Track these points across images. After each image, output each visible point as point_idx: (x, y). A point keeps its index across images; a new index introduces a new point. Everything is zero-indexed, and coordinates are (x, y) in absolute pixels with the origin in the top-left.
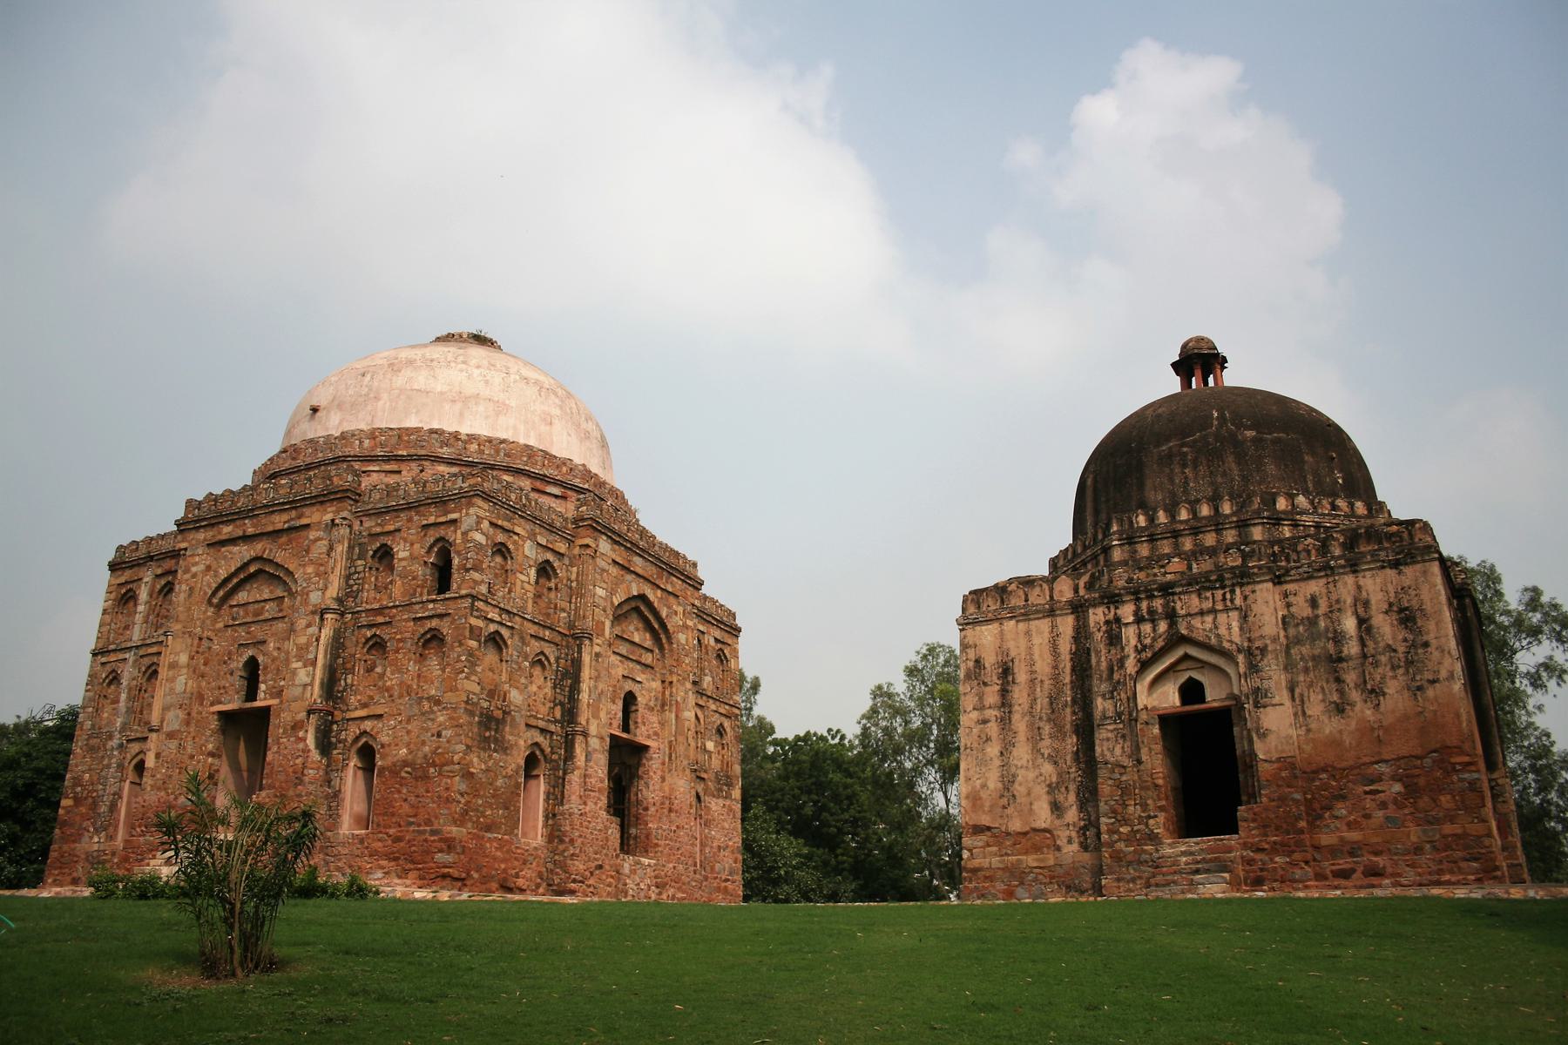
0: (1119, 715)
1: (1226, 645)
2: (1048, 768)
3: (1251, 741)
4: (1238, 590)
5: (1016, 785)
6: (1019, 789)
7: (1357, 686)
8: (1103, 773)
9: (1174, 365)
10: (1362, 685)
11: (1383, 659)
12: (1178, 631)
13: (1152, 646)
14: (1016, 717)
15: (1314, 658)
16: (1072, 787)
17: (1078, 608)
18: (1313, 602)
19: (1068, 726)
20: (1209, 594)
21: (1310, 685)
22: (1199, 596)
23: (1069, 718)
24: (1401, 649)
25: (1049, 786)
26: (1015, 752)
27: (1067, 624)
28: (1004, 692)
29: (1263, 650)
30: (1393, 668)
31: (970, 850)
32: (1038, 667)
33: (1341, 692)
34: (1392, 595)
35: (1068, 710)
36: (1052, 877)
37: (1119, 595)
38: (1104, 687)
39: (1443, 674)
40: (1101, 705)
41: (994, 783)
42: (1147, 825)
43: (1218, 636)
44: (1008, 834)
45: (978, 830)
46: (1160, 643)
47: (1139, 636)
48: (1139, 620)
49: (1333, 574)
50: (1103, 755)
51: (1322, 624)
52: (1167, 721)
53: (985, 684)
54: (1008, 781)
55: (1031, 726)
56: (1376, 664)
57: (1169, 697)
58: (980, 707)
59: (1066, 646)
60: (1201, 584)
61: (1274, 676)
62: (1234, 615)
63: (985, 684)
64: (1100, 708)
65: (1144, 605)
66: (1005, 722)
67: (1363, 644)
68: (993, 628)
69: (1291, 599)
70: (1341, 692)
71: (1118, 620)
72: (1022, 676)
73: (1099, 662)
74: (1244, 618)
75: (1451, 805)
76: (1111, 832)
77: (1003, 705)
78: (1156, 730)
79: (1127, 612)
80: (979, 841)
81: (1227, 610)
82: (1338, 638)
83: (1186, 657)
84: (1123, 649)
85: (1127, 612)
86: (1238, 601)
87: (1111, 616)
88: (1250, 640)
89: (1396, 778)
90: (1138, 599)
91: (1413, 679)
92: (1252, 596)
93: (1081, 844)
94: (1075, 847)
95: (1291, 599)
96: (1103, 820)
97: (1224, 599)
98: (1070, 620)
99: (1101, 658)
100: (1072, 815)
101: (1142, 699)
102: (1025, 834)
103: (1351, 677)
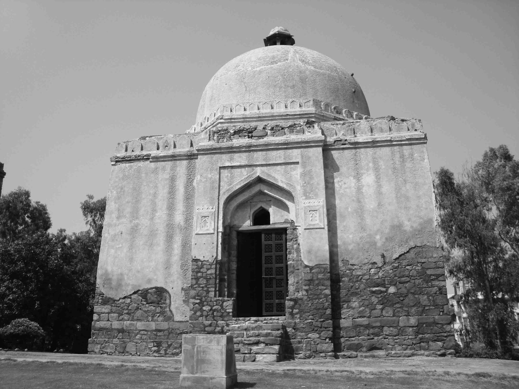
9: (265, 40)
80: (106, 309)
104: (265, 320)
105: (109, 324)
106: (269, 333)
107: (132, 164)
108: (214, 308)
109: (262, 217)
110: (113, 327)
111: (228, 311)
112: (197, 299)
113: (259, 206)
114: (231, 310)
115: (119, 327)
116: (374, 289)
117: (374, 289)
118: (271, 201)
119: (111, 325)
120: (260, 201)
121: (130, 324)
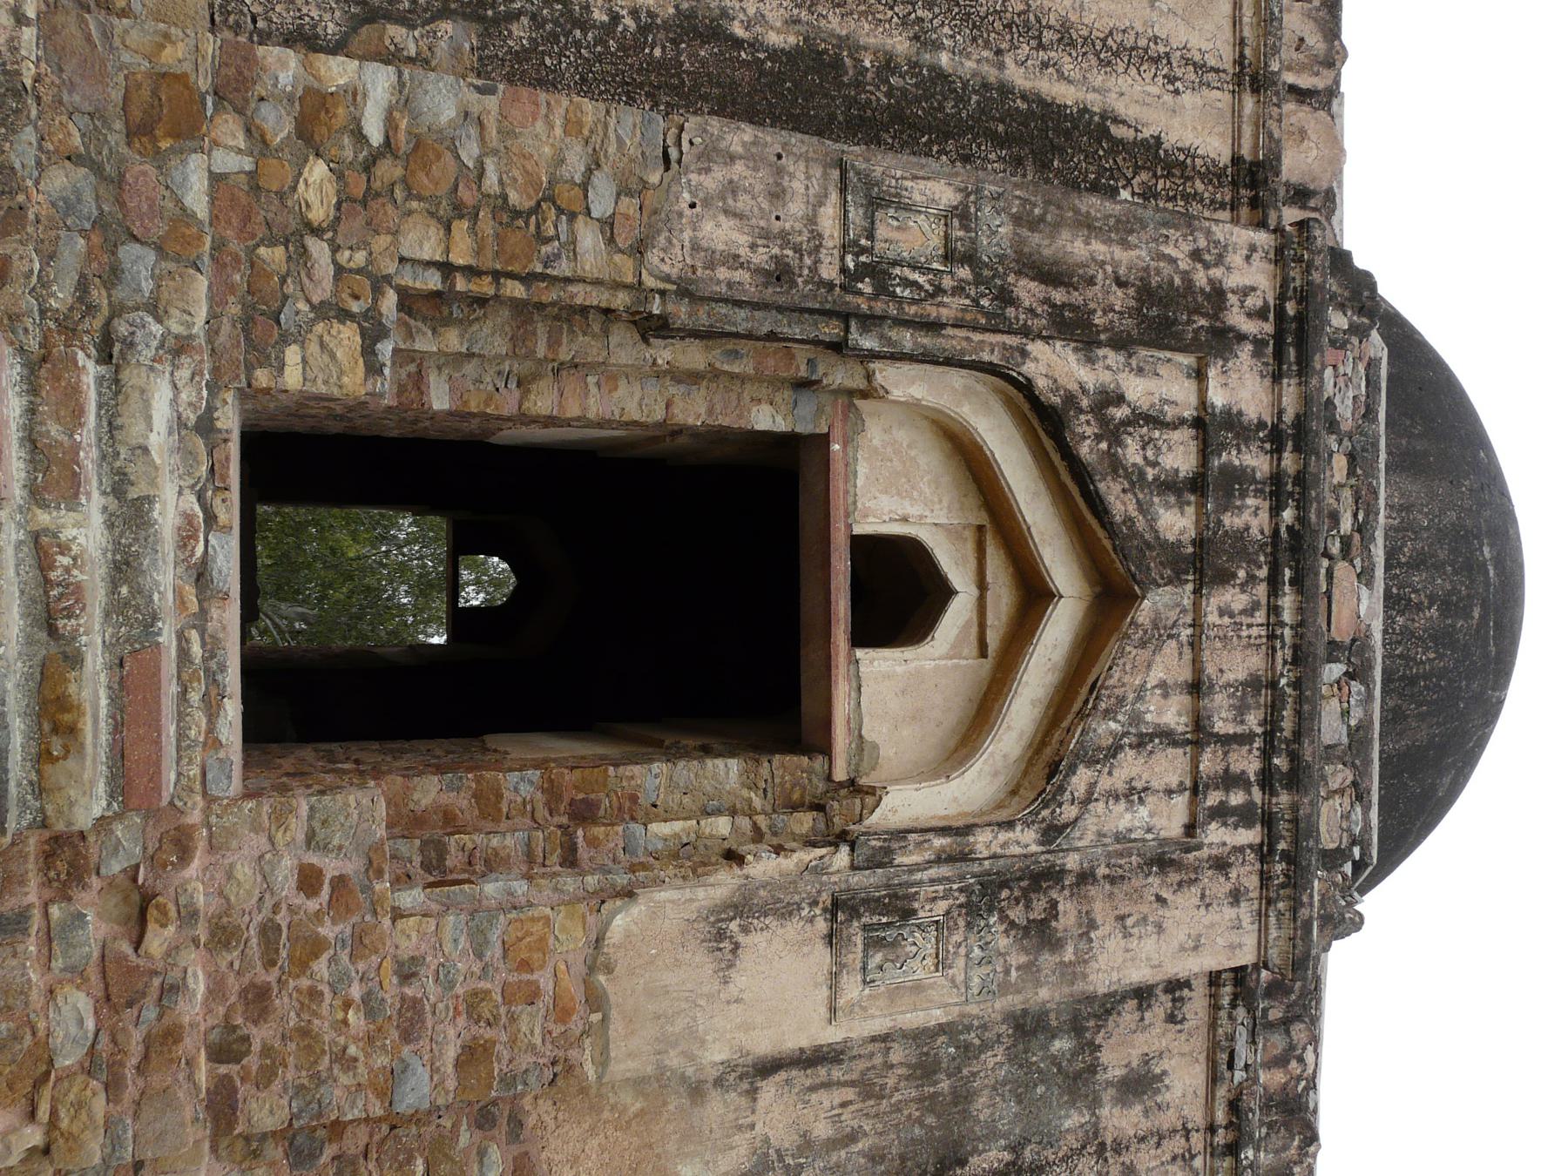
0: (878, 272)
1: (1081, 779)
3: (691, 859)
4: (1249, 836)
8: (630, 128)
12: (1148, 584)
13: (1115, 465)
15: (962, 1097)
18: (1140, 1084)
19: (834, 23)
20: (1253, 721)
21: (868, 1089)
22: (1252, 684)
27: (1198, 126)
29: (1041, 934)
35: (900, 44)
37: (1304, 369)
38: (996, 233)
40: (926, 197)
43: (1115, 750)
46: (1119, 501)
47: (1151, 419)
48: (1208, 427)
49: (1213, 1151)
50: (711, 155)
51: (1074, 1119)
57: (888, 488)
60: (1285, 699)
61: (939, 983)
62: (1170, 818)
64: (918, 191)
65: (1256, 461)
69: (1161, 1005)
71: (1222, 341)
73: (1087, 225)
74: (1161, 861)
76: (316, 116)
78: (766, 418)
79: (1242, 388)
81: (1196, 789)
83: (1034, 596)
84: (1121, 343)
85: (1242, 388)
86: (1216, 835)
87: (1237, 319)
88: (1086, 877)
90: (1276, 438)
92: (1219, 887)
95: (1161, 1005)
96: (379, 82)
97: (1230, 780)
98: (1214, 146)
99: (1105, 250)
101: (907, 384)
108: (318, 249)
109: (898, 593)
111: (292, 354)
112: (390, 124)
114: (293, 378)
118: (983, 653)
120: (982, 585)
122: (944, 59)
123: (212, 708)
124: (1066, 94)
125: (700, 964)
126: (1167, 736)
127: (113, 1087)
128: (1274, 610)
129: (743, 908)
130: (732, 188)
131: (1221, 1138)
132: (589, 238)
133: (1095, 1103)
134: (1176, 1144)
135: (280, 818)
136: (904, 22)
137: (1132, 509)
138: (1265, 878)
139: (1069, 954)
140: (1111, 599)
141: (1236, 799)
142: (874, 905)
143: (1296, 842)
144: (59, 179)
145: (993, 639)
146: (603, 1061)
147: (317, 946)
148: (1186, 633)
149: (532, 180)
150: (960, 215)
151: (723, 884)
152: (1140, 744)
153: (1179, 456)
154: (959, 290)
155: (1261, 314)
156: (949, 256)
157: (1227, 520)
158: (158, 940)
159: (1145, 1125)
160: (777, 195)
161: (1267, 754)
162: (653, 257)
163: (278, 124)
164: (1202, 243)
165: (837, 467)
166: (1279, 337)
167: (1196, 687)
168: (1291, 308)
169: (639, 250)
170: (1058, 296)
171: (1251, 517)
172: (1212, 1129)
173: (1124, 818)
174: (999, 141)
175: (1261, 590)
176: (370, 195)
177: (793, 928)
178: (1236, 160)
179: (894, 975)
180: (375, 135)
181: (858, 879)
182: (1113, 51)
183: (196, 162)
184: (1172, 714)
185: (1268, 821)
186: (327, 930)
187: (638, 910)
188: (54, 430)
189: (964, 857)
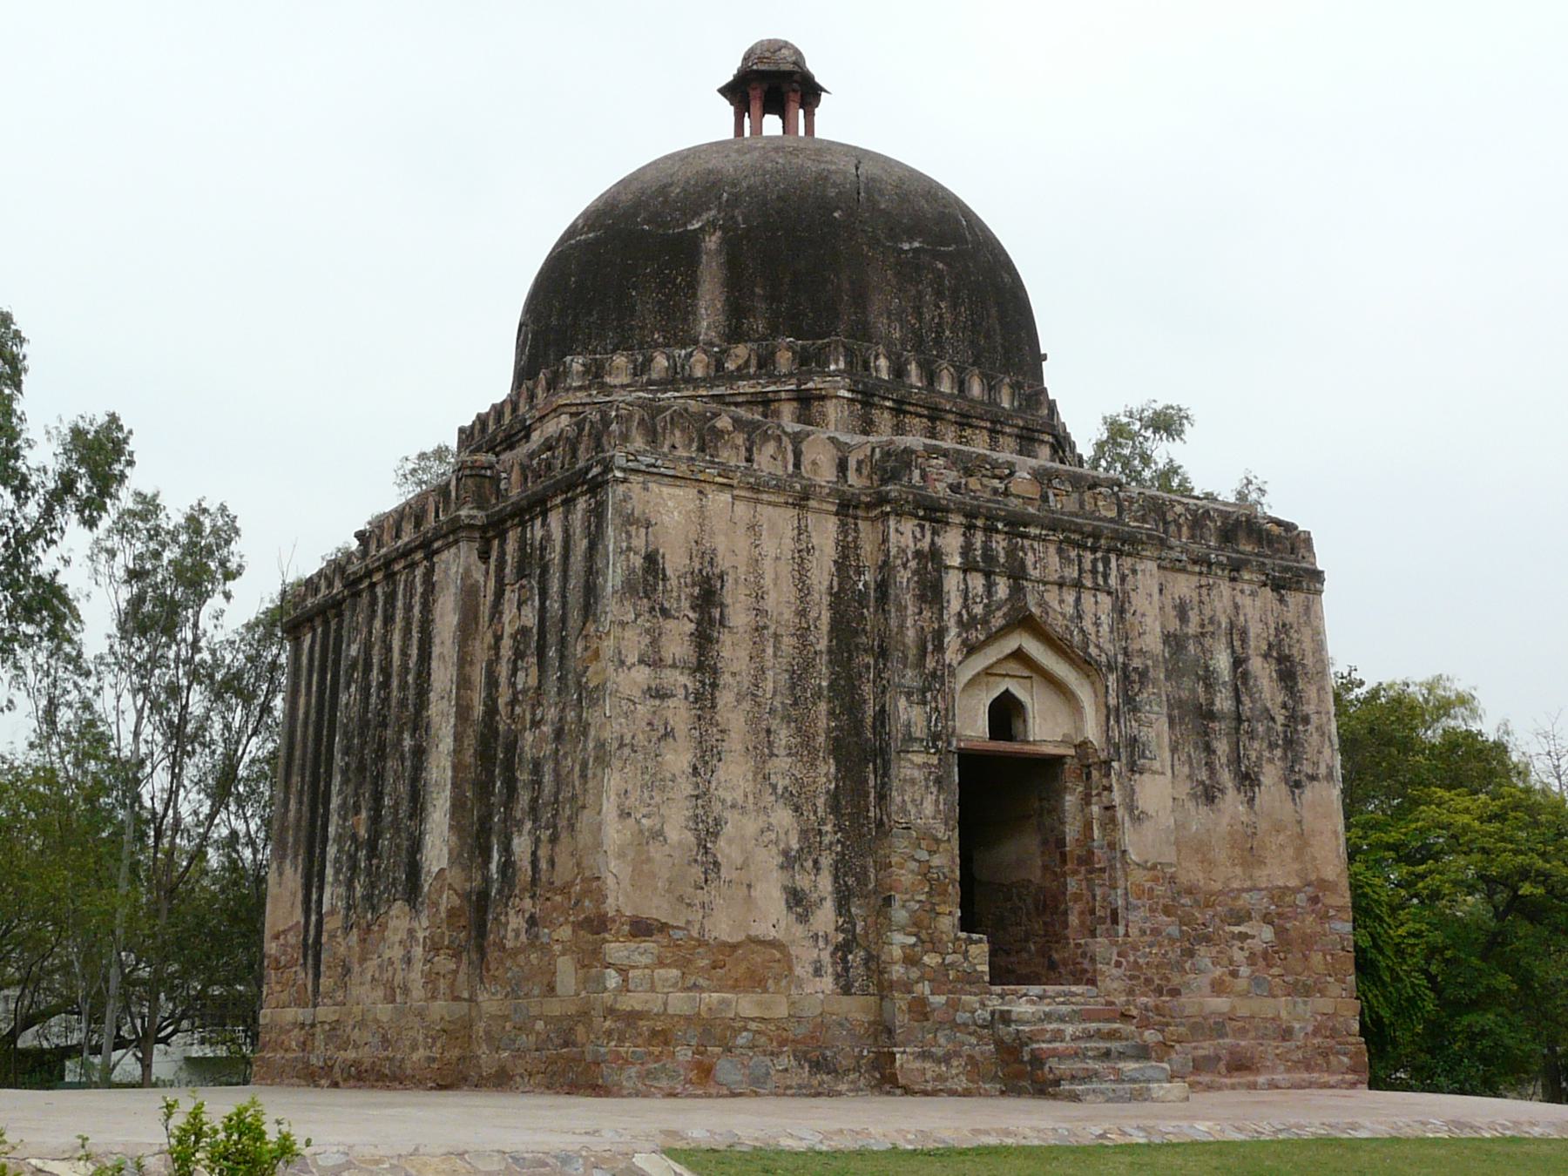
1: (1093, 650)
2: (783, 817)
5: (722, 842)
6: (725, 849)
7: (1230, 762)
10: (1236, 759)
11: (1260, 729)
14: (725, 698)
16: (826, 861)
17: (846, 507)
19: (821, 739)
20: (1073, 554)
22: (1060, 551)
23: (823, 723)
24: (1280, 719)
25: (785, 853)
26: (721, 773)
28: (704, 639)
29: (1143, 674)
30: (1272, 746)
31: (622, 971)
32: (770, 603)
33: (1210, 765)
34: (1272, 631)
35: (823, 707)
36: (783, 1043)
37: (947, 510)
38: (911, 678)
39: (1323, 770)
41: (678, 832)
42: (965, 954)
44: (701, 942)
45: (641, 928)
52: (971, 761)
53: (665, 613)
54: (707, 832)
55: (753, 721)
56: (1252, 735)
58: (654, 661)
59: (822, 574)
63: (665, 613)
66: (704, 700)
67: (1238, 701)
68: (687, 494)
70: (1210, 765)
71: (935, 554)
72: (739, 616)
73: (902, 626)
74: (1120, 610)
75: (1321, 969)
76: (910, 960)
77: (700, 667)
80: (640, 953)
81: (1096, 588)
82: (1208, 679)
85: (951, 541)
86: (1113, 581)
87: (925, 545)
89: (1267, 919)
90: (970, 528)
91: (1292, 769)
93: (837, 976)
94: (827, 983)
98: (832, 524)
99: (910, 622)
100: (825, 917)
102: (734, 947)
103: (1222, 747)
104: (1059, 995)
105: (660, 1002)
106: (1116, 1030)
107: (677, 491)
108: (949, 959)
109: (1006, 714)
110: (670, 1011)
111: (979, 968)
112: (910, 934)
113: (1002, 689)
114: (986, 968)
115: (686, 1010)
116: (1236, 929)
117: (1236, 929)
119: (665, 1004)
121: (722, 1002)
122: (824, 684)
123: (1074, 994)
124: (826, 616)
125: (1147, 824)
126: (1078, 600)
127: (1168, 1024)
128: (1034, 538)
129: (1131, 807)
130: (913, 801)
131: (1204, 569)
132: (936, 861)
133: (1187, 636)
134: (1204, 591)
135: (1102, 973)
136: (814, 704)
137: (999, 614)
138: (1129, 555)
139: (1150, 663)
140: (1024, 621)
141: (1100, 568)
142: (1132, 754)
143: (1118, 539)
144: (942, 1041)
145: (1026, 673)
146: (1171, 865)
147: (1136, 962)
148: (1042, 588)
149: (921, 882)
150: (909, 695)
151: (1121, 813)
152: (1080, 617)
153: (977, 582)
154: (935, 699)
155: (922, 527)
156: (924, 703)
157: (1002, 560)
158: (1134, 1012)
159: (1196, 610)
160: (913, 782)
161: (1085, 548)
162: (940, 835)
163: (915, 973)
164: (899, 562)
165: (969, 745)
166: (932, 520)
167: (1061, 585)
168: (921, 513)
169: (937, 841)
170: (930, 647)
171: (1000, 544)
172: (1201, 573)
173: (1105, 629)
174: (850, 658)
175: (1027, 543)
176: (932, 942)
177: (1137, 788)
178: (837, 514)
179: (1153, 746)
180: (913, 940)
181: (1124, 761)
182: (804, 590)
183: (932, 999)
184: (1070, 598)
185: (1109, 551)
186: (1132, 959)
187: (1130, 850)
188: (1048, 1036)
189: (1117, 709)
